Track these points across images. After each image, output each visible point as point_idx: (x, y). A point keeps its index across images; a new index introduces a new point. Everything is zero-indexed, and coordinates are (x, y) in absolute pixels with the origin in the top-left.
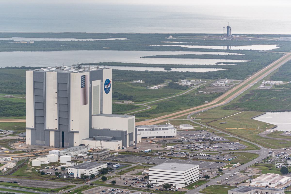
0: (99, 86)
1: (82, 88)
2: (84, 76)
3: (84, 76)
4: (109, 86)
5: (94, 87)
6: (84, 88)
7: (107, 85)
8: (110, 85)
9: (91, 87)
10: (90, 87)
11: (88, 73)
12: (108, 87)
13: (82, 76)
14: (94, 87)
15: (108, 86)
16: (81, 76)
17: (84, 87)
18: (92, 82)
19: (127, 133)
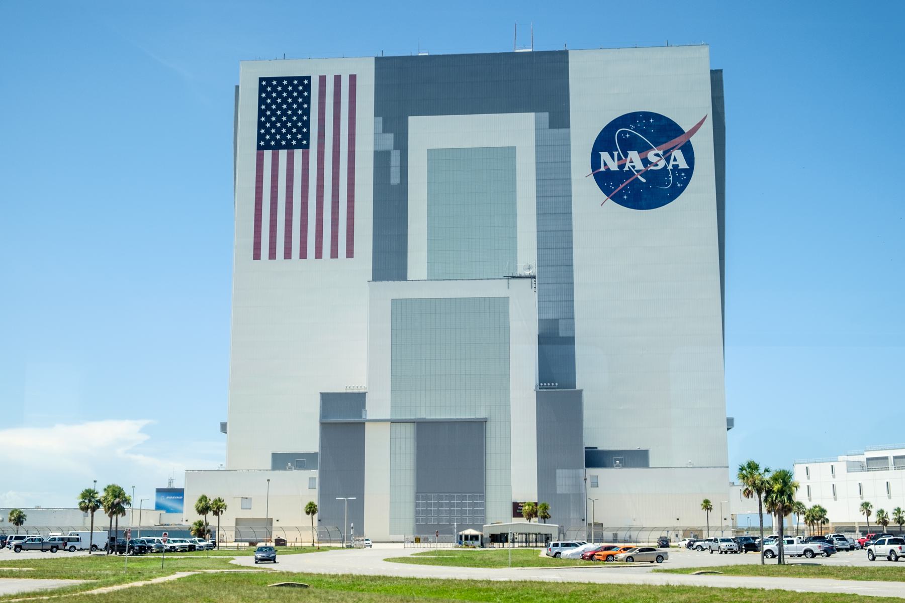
0: (510, 152)
1: (268, 154)
2: (309, 78)
3: (309, 78)
4: (667, 157)
5: (435, 156)
6: (298, 153)
7: (634, 155)
8: (678, 154)
9: (395, 157)
10: (381, 159)
12: (645, 162)
13: (280, 80)
14: (433, 154)
15: (651, 156)
16: (261, 80)
17: (307, 147)
18: (416, 124)
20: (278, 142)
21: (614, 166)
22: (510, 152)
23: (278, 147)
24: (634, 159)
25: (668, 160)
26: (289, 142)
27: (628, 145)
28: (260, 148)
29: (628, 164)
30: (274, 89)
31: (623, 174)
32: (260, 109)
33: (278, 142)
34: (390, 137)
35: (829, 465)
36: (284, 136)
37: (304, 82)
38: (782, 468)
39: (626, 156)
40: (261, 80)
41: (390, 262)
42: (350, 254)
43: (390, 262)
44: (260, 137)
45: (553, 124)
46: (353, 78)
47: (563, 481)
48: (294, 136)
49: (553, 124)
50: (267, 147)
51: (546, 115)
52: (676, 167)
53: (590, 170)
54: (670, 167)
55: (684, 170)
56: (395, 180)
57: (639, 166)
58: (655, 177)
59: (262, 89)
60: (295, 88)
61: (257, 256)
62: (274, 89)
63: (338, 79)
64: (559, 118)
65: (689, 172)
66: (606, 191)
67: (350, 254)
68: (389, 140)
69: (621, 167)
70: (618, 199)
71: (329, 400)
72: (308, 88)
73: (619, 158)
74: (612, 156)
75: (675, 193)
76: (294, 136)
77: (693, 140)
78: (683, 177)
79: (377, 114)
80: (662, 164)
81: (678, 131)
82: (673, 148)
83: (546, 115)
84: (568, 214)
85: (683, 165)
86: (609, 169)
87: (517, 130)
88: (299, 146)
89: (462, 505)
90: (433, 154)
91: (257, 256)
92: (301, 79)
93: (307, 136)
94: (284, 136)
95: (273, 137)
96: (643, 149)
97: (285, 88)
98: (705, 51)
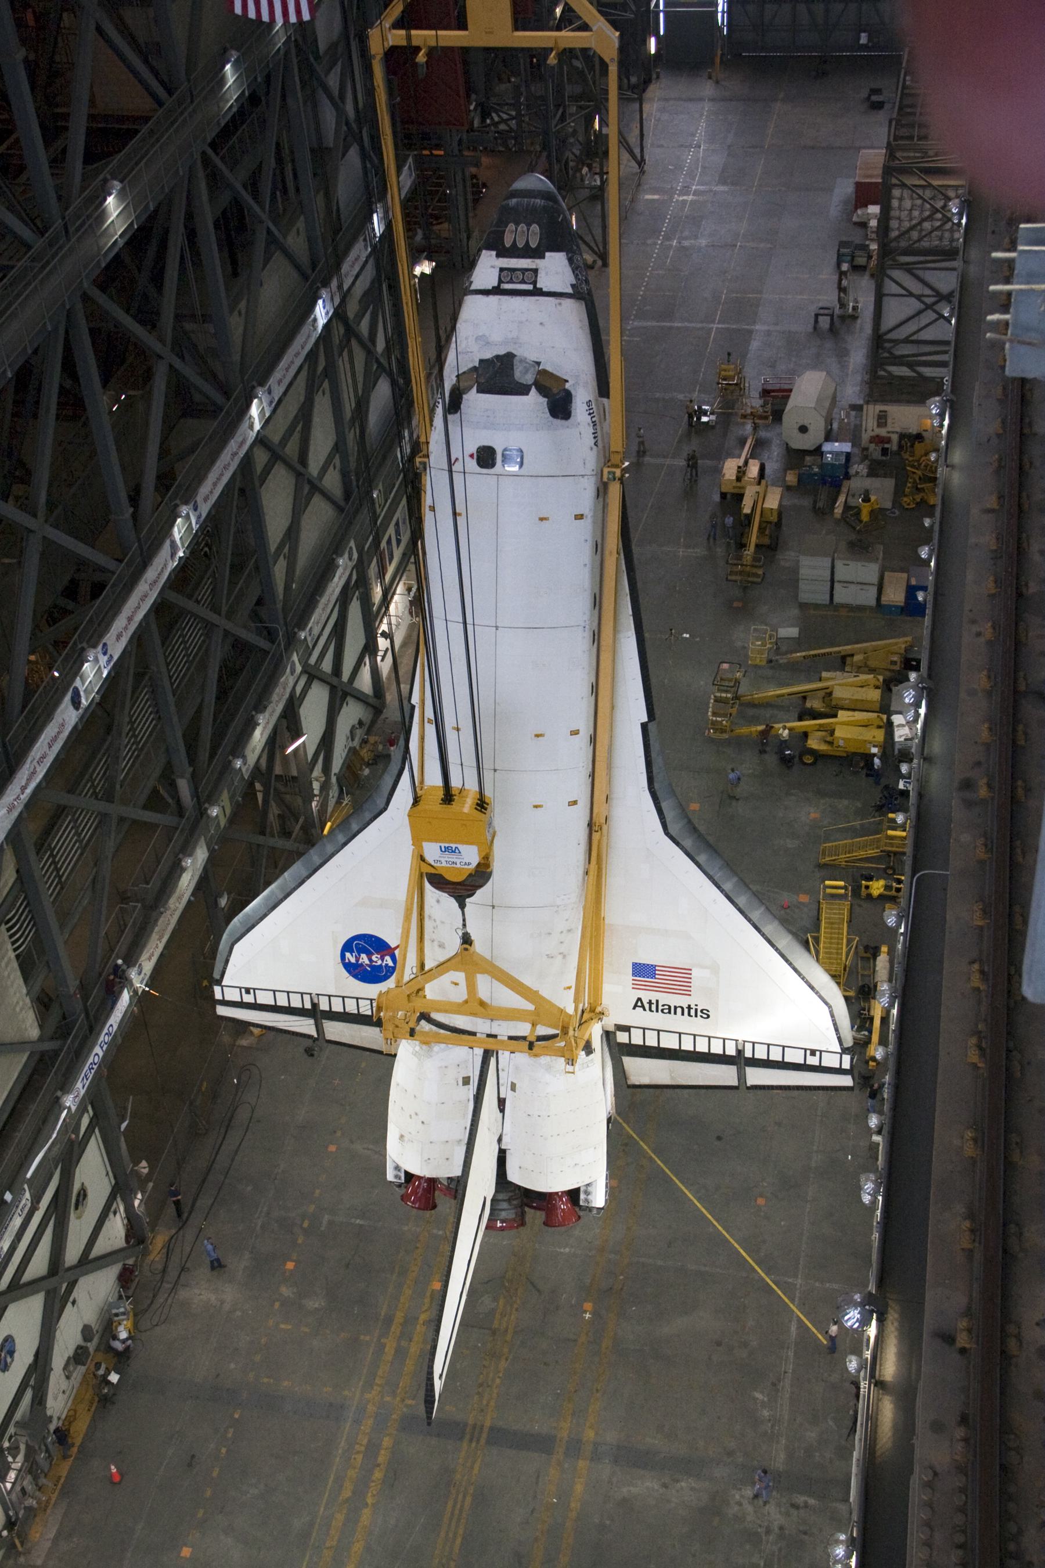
7: (363, 956)
8: (388, 958)
12: (371, 960)
15: (374, 958)
21: (353, 960)
24: (364, 959)
27: (361, 950)
52: (387, 965)
57: (367, 962)
65: (394, 969)
66: (349, 971)
69: (357, 959)
70: (355, 976)
80: (380, 962)
85: (391, 964)
96: (369, 955)
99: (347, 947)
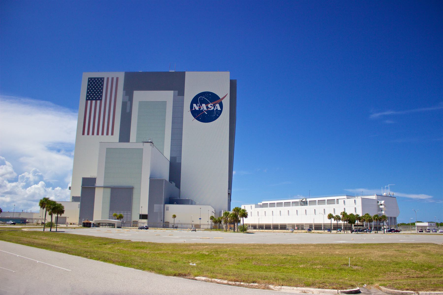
0: (164, 104)
1: (89, 102)
2: (104, 78)
3: (104, 78)
6: (98, 102)
7: (204, 105)
8: (218, 105)
10: (124, 105)
11: (121, 76)
12: (207, 107)
13: (95, 78)
14: (140, 102)
15: (209, 106)
16: (89, 78)
17: (101, 100)
19: (99, 183)
20: (93, 98)
21: (197, 108)
22: (164, 104)
23: (92, 99)
25: (214, 107)
26: (96, 98)
27: (202, 102)
28: (87, 100)
29: (202, 108)
30: (93, 81)
31: (200, 111)
32: (88, 87)
33: (93, 98)
34: (128, 97)
35: (250, 205)
36: (94, 96)
37: (102, 79)
38: (237, 206)
39: (201, 105)
40: (89, 78)
41: (125, 136)
42: (112, 134)
43: (125, 136)
44: (87, 96)
45: (179, 95)
46: (117, 79)
47: (156, 207)
48: (98, 96)
49: (179, 95)
50: (89, 99)
51: (177, 91)
52: (217, 109)
53: (190, 110)
54: (215, 109)
55: (219, 110)
56: (128, 111)
57: (205, 109)
58: (210, 112)
59: (89, 81)
60: (99, 81)
61: (83, 134)
62: (93, 81)
63: (113, 79)
64: (181, 92)
65: (221, 111)
66: (194, 116)
67: (112, 134)
68: (127, 98)
69: (200, 109)
70: (198, 119)
71: (85, 180)
72: (103, 81)
73: (199, 106)
74: (197, 106)
75: (216, 118)
76: (98, 96)
77: (223, 101)
78: (219, 113)
79: (124, 90)
81: (220, 98)
82: (216, 103)
83: (177, 91)
84: (182, 123)
85: (219, 109)
86: (195, 109)
87: (167, 96)
88: (99, 99)
89: (127, 215)
90: (140, 102)
91: (83, 134)
92: (101, 78)
93: (101, 96)
94: (94, 96)
95: (91, 96)
96: (207, 103)
97: (96, 81)
98: (228, 73)
99: (195, 101)
